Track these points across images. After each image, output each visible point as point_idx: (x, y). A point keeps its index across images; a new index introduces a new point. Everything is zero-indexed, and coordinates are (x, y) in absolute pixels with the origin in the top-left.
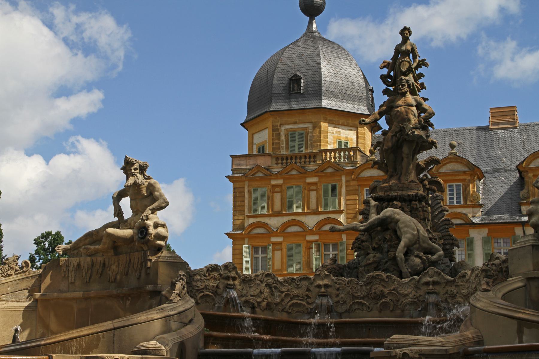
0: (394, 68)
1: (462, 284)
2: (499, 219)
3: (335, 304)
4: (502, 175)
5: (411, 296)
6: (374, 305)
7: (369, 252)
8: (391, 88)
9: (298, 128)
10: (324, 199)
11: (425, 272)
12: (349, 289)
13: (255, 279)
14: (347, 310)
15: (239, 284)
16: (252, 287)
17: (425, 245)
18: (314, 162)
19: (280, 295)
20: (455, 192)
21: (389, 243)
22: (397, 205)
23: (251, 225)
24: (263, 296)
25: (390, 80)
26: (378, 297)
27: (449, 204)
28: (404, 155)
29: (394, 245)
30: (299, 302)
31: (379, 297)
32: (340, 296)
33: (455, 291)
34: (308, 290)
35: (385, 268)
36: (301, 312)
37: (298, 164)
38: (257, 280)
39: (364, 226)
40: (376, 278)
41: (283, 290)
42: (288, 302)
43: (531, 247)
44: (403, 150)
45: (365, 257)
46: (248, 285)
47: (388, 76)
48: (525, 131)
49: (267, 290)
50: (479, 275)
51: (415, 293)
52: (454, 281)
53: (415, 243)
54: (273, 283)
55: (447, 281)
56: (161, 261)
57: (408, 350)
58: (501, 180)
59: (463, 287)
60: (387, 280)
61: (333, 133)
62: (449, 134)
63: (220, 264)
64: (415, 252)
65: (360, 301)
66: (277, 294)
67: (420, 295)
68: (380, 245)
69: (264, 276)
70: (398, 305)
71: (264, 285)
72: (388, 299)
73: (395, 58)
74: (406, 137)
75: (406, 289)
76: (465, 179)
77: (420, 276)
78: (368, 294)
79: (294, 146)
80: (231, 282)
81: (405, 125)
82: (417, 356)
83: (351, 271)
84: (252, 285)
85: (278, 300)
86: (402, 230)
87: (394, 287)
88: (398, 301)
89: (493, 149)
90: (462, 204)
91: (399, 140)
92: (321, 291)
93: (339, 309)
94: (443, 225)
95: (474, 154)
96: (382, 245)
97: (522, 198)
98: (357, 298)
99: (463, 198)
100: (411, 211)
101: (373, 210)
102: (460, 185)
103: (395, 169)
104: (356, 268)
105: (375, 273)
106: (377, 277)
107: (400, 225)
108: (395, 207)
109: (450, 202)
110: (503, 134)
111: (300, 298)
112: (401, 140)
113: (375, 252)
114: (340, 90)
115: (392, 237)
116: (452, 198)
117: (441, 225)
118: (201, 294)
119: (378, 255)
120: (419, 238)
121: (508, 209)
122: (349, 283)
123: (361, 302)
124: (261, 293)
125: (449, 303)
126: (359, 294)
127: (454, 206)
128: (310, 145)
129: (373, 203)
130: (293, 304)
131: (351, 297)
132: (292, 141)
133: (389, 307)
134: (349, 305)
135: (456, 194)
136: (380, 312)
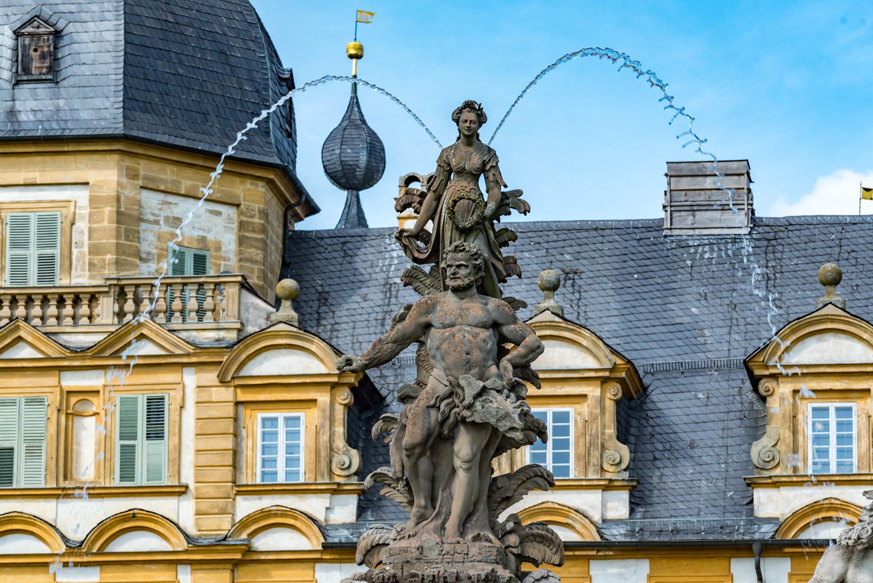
0: (435, 212)
2: (686, 532)
4: (700, 387)
8: (427, 268)
9: (40, 202)
10: (122, 446)
18: (90, 318)
28: (457, 463)
37: (37, 322)
44: (456, 447)
47: (420, 234)
48: (774, 242)
58: (695, 402)
61: (157, 222)
62: (537, 240)
74: (466, 413)
79: (24, 260)
89: (671, 299)
90: (572, 476)
95: (615, 313)
97: (756, 463)
99: (578, 458)
103: (433, 499)
110: (707, 248)
112: (452, 419)
114: (185, 79)
121: (713, 496)
128: (78, 260)
132: (14, 245)
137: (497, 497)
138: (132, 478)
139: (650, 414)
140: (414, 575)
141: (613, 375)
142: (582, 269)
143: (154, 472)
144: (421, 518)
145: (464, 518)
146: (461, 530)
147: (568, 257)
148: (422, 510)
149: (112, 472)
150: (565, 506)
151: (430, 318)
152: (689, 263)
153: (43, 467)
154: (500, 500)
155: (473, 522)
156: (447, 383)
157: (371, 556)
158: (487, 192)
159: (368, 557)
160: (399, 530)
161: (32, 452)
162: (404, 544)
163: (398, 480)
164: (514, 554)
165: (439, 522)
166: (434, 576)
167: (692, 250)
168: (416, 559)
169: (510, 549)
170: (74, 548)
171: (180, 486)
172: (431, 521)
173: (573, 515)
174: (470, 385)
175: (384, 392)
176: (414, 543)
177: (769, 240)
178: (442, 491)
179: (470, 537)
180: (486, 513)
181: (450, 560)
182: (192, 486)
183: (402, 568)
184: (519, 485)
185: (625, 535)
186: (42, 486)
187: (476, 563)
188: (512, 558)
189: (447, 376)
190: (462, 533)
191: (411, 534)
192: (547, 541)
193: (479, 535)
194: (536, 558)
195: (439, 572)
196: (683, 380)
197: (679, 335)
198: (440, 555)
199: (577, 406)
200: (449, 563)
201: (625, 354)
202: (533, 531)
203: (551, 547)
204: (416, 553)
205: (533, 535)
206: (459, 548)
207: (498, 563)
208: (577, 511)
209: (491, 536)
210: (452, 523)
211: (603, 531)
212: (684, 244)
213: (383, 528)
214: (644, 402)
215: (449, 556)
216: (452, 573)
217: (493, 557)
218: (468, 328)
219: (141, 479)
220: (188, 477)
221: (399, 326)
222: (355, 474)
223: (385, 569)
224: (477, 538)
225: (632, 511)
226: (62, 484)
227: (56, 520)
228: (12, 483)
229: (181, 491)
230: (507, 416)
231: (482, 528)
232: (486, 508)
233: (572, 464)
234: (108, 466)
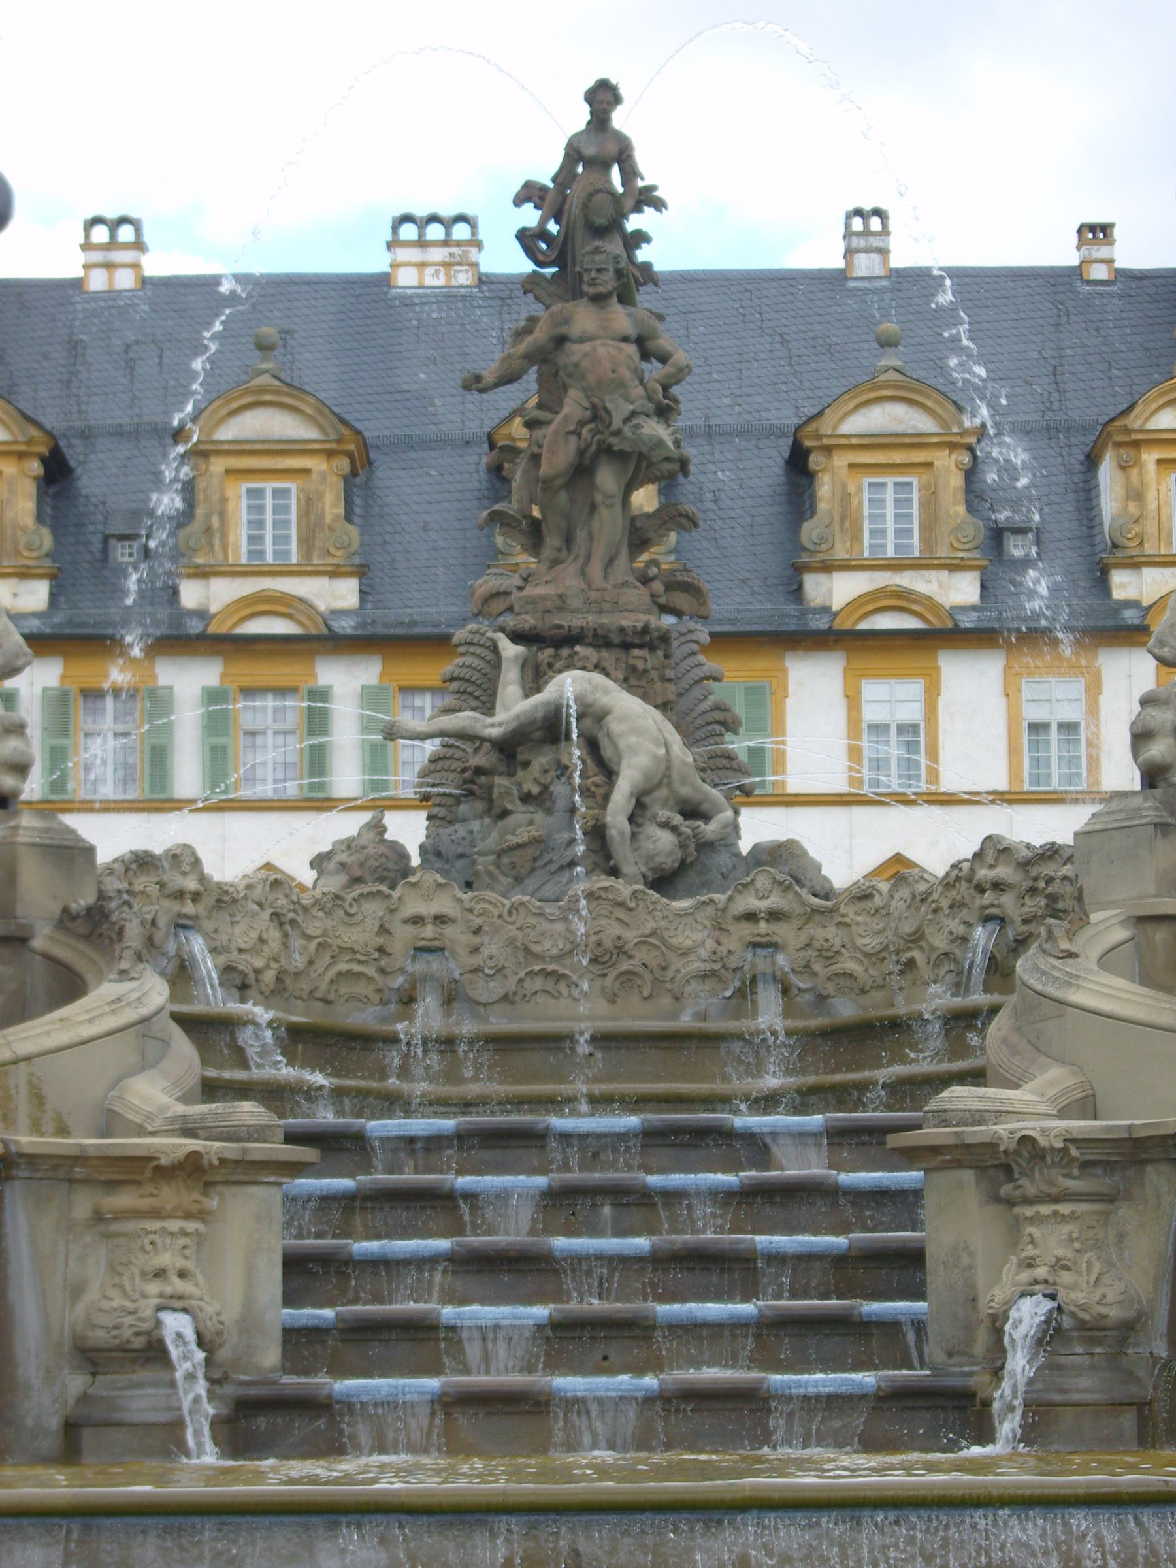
1: (859, 918)
3: (467, 976)
7: (509, 807)
12: (512, 931)
13: (245, 898)
15: (205, 913)
16: (238, 922)
17: (685, 791)
19: (305, 948)
20: (269, 517)
22: (586, 658)
24: (266, 949)
25: (544, 246)
27: (249, 559)
30: (356, 968)
32: (485, 952)
33: (837, 942)
34: (383, 930)
36: (360, 1001)
39: (500, 724)
40: (599, 898)
41: (310, 932)
47: (541, 234)
48: (509, 302)
49: (274, 935)
50: (935, 896)
53: (659, 785)
55: (813, 910)
56: (25, 844)
57: (1034, 1129)
63: (158, 850)
64: (660, 814)
65: (550, 967)
66: (297, 943)
67: (730, 952)
70: (664, 981)
71: (266, 915)
72: (636, 962)
73: (564, 177)
74: (613, 440)
75: (688, 933)
76: (306, 472)
80: (189, 908)
81: (612, 401)
83: (447, 867)
85: (298, 961)
86: (622, 744)
88: (664, 969)
89: (397, 363)
91: (588, 447)
92: (422, 935)
93: (480, 991)
94: (709, 723)
95: (334, 378)
96: (552, 788)
97: (501, 548)
98: (539, 957)
100: (626, 680)
102: (288, 491)
104: (461, 856)
105: (596, 881)
106: (603, 894)
107: (614, 725)
108: (580, 664)
110: (434, 307)
111: (358, 956)
112: (593, 448)
113: (531, 809)
116: (260, 539)
117: (700, 721)
119: (539, 817)
120: (668, 768)
122: (514, 912)
123: (554, 972)
124: (262, 940)
125: (815, 974)
126: (547, 945)
127: (266, 569)
129: (510, 650)
130: (340, 974)
131: (521, 954)
134: (516, 978)
135: (275, 523)
136: (612, 1001)
139: (378, 492)
140: (559, 627)
141: (340, 448)
142: (294, 327)
147: (277, 314)
151: (564, 330)
152: (415, 323)
156: (587, 405)
158: (623, 185)
160: (525, 575)
166: (582, 628)
167: (418, 309)
174: (619, 409)
175: (72, 464)
177: (502, 299)
185: (355, 628)
189: (588, 398)
196: (413, 455)
197: (407, 404)
199: (300, 482)
201: (353, 423)
204: (558, 603)
210: (596, 569)
211: (330, 622)
212: (407, 302)
214: (368, 479)
218: (611, 342)
221: (530, 339)
222: (47, 555)
225: (362, 600)
230: (660, 443)
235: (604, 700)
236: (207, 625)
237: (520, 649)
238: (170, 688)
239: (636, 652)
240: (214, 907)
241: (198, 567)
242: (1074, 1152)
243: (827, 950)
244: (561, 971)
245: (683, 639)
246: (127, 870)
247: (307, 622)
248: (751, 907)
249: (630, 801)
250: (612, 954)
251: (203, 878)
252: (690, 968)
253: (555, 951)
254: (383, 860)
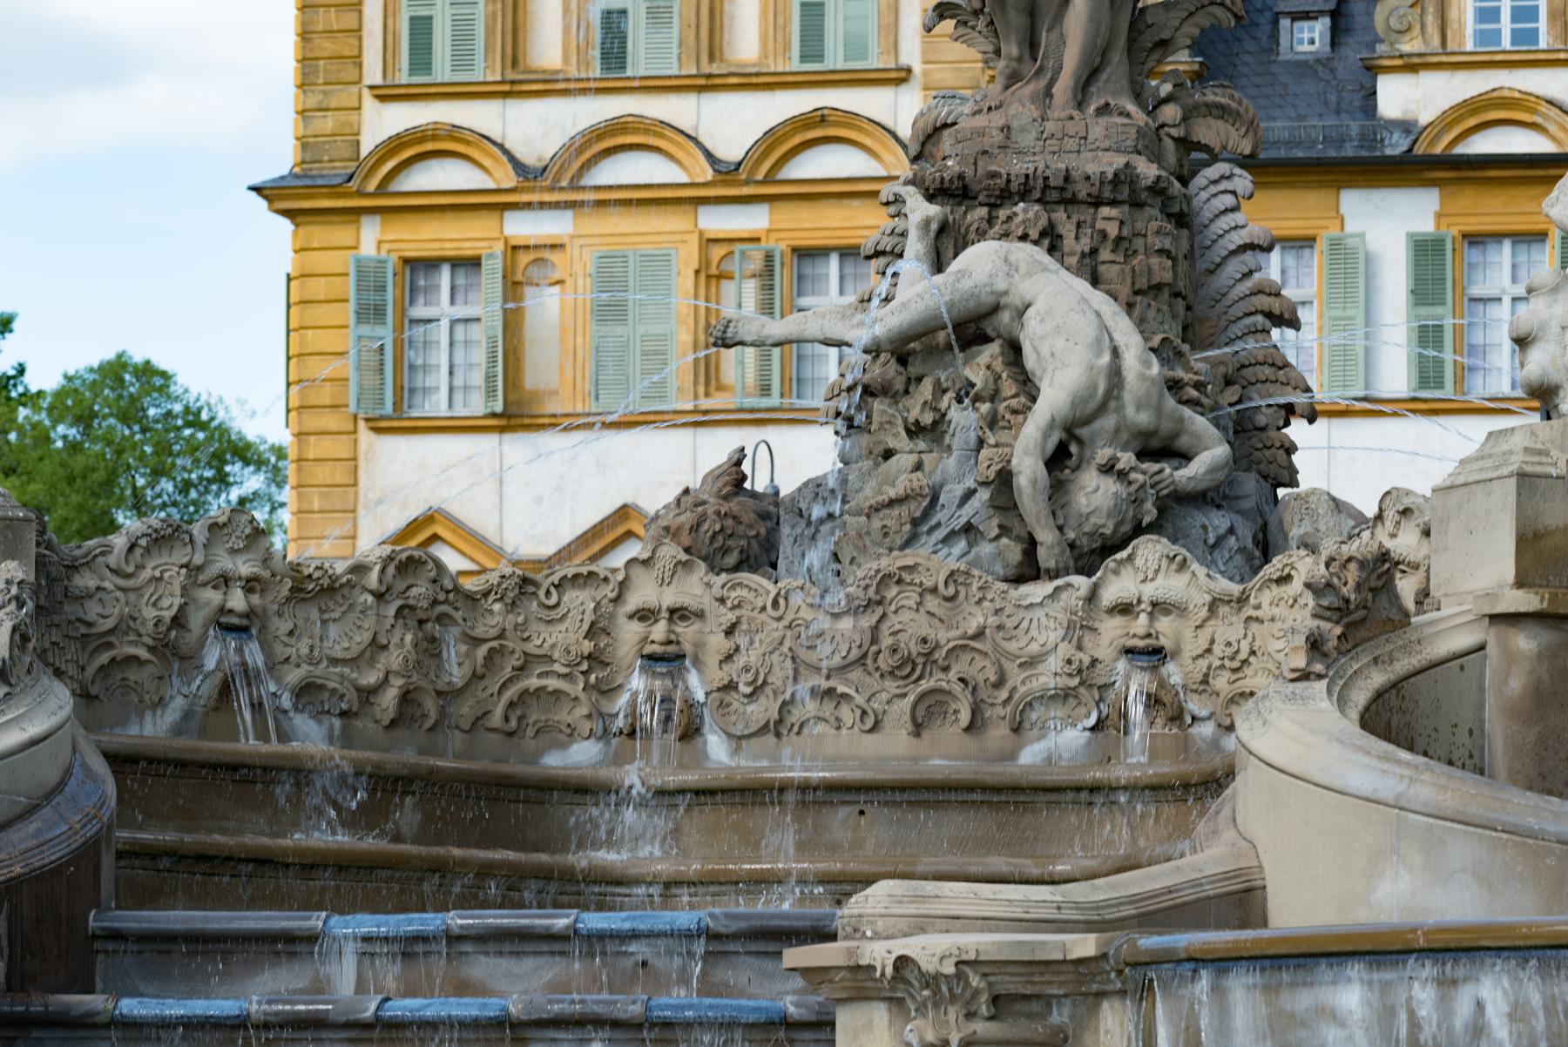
1: (1276, 611)
3: (715, 695)
5: (1054, 663)
6: (888, 702)
7: (892, 444)
11: (1118, 556)
14: (768, 721)
21: (985, 407)
23: (395, 144)
26: (908, 670)
29: (1008, 416)
30: (553, 683)
31: (913, 670)
32: (741, 660)
33: (1245, 647)
35: (963, 521)
38: (357, 590)
40: (900, 582)
41: (480, 631)
42: (504, 686)
43: (1513, 481)
45: (877, 465)
46: (314, 614)
51: (1073, 651)
52: (1242, 600)
54: (435, 602)
59: (1279, 625)
60: (951, 591)
64: (1100, 452)
67: (1094, 662)
68: (944, 415)
69: (391, 570)
70: (992, 705)
71: (391, 610)
72: (953, 675)
77: (1099, 574)
78: (865, 655)
82: (949, 969)
84: (333, 615)
85: (456, 673)
87: (981, 620)
88: (999, 684)
90: (1543, 45)
93: (733, 718)
101: (915, 246)
106: (907, 577)
109: (1482, 37)
111: (557, 667)
115: (998, 378)
118: (104, 658)
122: (782, 602)
123: (830, 692)
124: (377, 646)
129: (920, 210)
131: (788, 663)
133: (956, 712)
137: (1147, 40)
138: (819, 57)
140: (994, 175)
143: (855, 46)
144: (1013, 78)
145: (1085, 76)
146: (1080, 96)
148: (1014, 64)
149: (787, 47)
150: (1530, 94)
153: (676, 41)
154: (1150, 45)
155: (1100, 84)
157: (933, 145)
159: (929, 147)
161: (657, 15)
162: (980, 121)
163: (977, 13)
164: (1173, 138)
165: (1043, 83)
166: (1027, 176)
168: (999, 147)
169: (1166, 129)
170: (726, 172)
171: (899, 69)
172: (1028, 82)
173: (1544, 110)
176: (997, 119)
178: (1048, 31)
179: (1091, 109)
180: (1125, 68)
181: (1056, 149)
182: (917, 68)
183: (975, 163)
184: (1183, 20)
186: (675, 72)
187: (1100, 153)
188: (1169, 145)
190: (1080, 105)
191: (993, 105)
192: (1230, 115)
193: (1107, 105)
194: (1212, 145)
195: (1036, 169)
198: (1039, 139)
200: (1054, 153)
202: (1206, 99)
203: (1237, 125)
204: (998, 138)
205: (1208, 106)
206: (1071, 128)
207: (1139, 153)
208: (1550, 102)
209: (1131, 107)
210: (1063, 86)
213: (954, 97)
215: (1054, 142)
216: (1057, 169)
217: (1129, 143)
219: (835, 58)
220: (911, 51)
223: (945, 165)
224: (1104, 110)
226: (706, 69)
227: (696, 129)
228: (625, 68)
229: (899, 77)
231: (1115, 94)
232: (1125, 59)
233: (1543, 24)
234: (780, 38)
235: (1024, 288)
236: (1415, 142)
237: (933, 210)
238: (1362, 236)
239: (1105, 211)
240: (288, 599)
241: (1401, 56)
242: (975, 981)
243: (1232, 659)
244: (841, 689)
245: (1213, 189)
246: (132, 548)
247: (1560, 135)
248: (1125, 594)
249: (1046, 435)
250: (915, 665)
251: (267, 560)
252: (1035, 685)
253: (837, 660)
254: (729, 522)
